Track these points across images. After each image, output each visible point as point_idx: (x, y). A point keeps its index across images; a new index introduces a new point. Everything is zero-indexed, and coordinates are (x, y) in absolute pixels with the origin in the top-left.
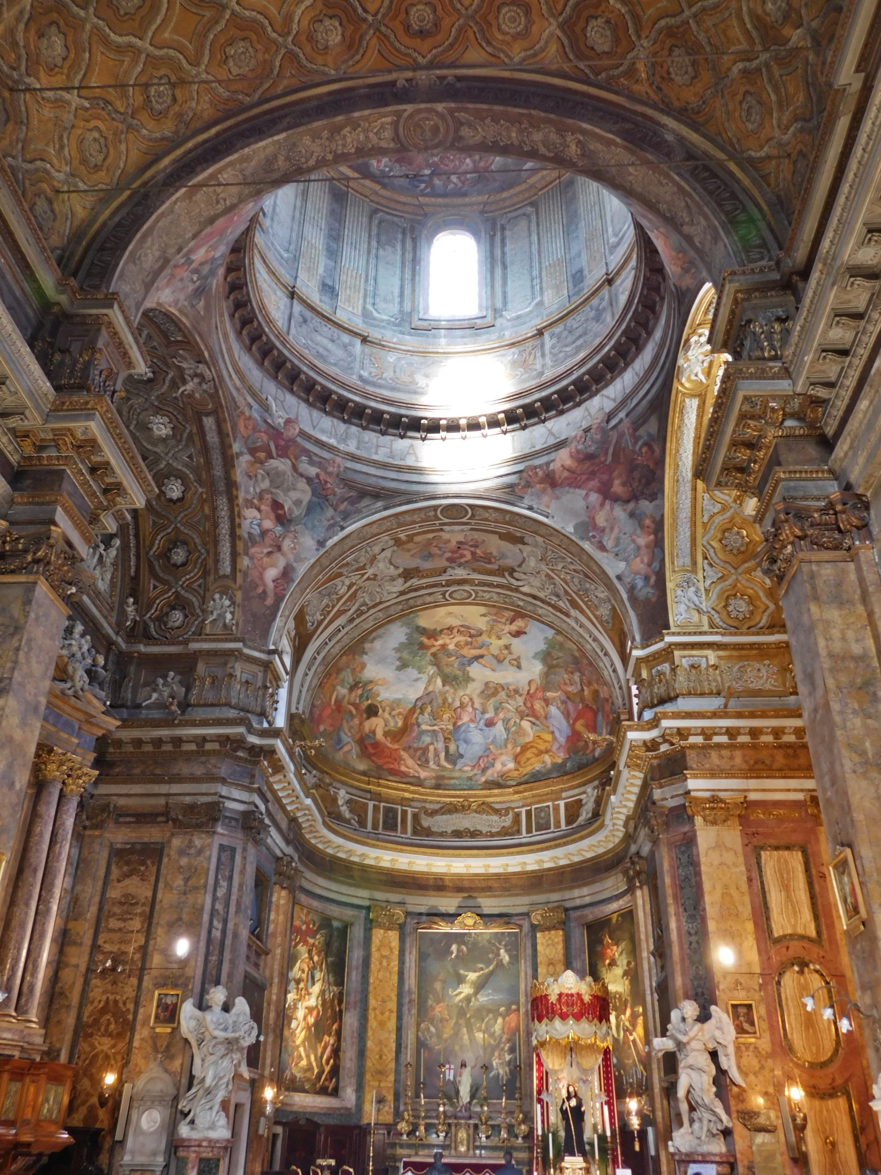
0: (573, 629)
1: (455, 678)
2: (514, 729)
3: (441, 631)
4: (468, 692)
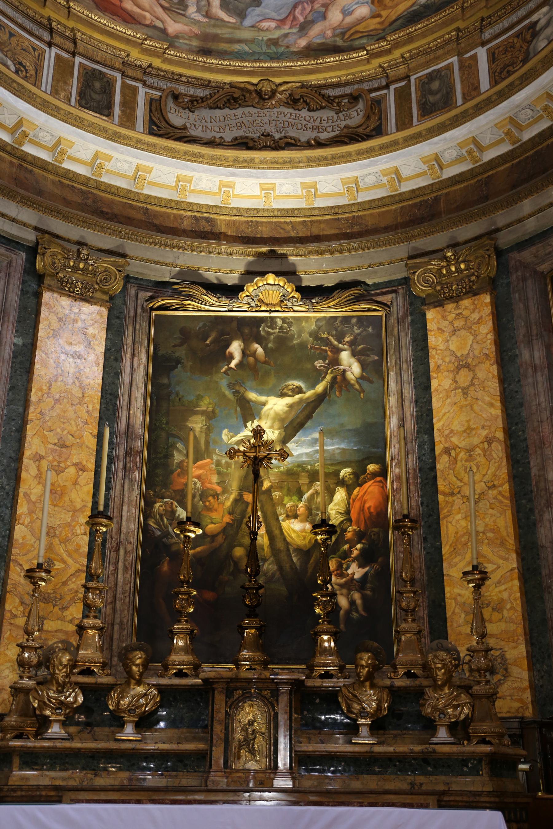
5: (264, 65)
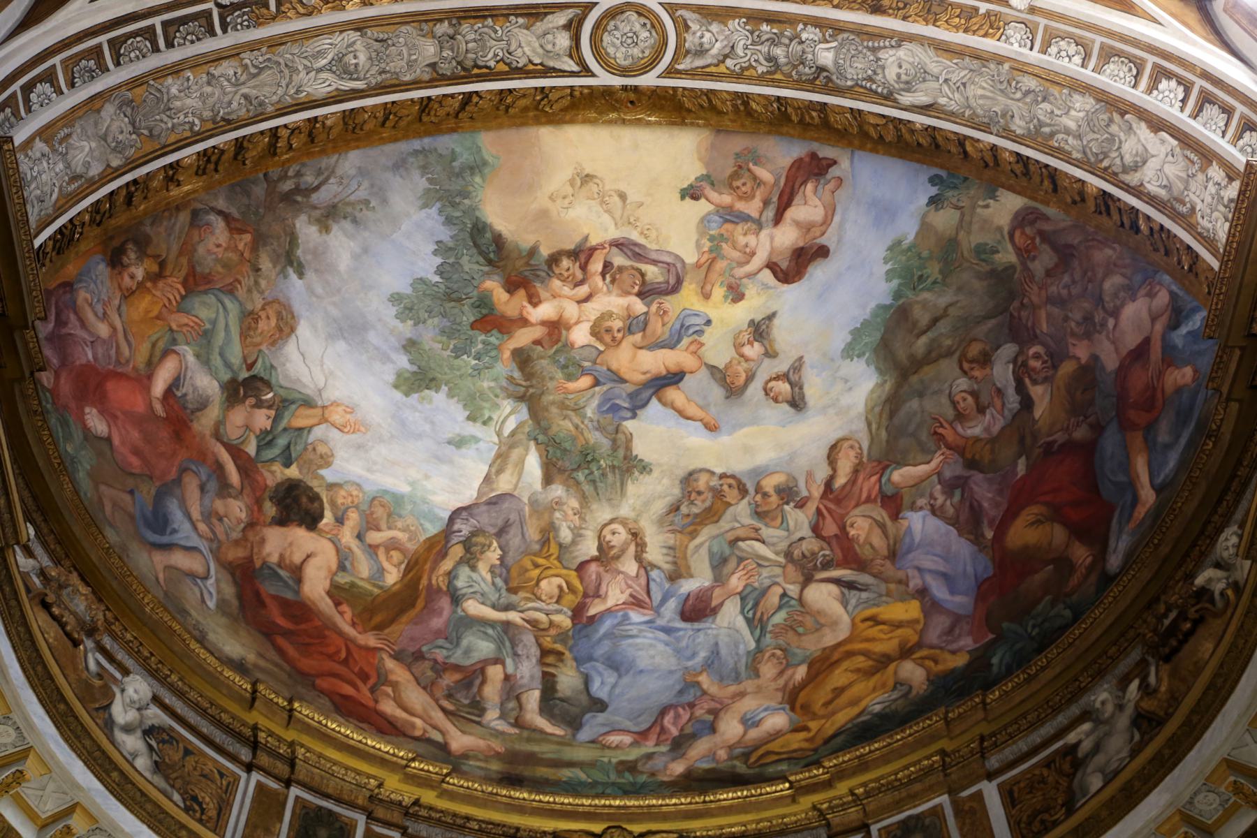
0: (1020, 68)
1: (587, 458)
2: (779, 618)
3: (554, 260)
4: (625, 511)
5: (612, 802)
